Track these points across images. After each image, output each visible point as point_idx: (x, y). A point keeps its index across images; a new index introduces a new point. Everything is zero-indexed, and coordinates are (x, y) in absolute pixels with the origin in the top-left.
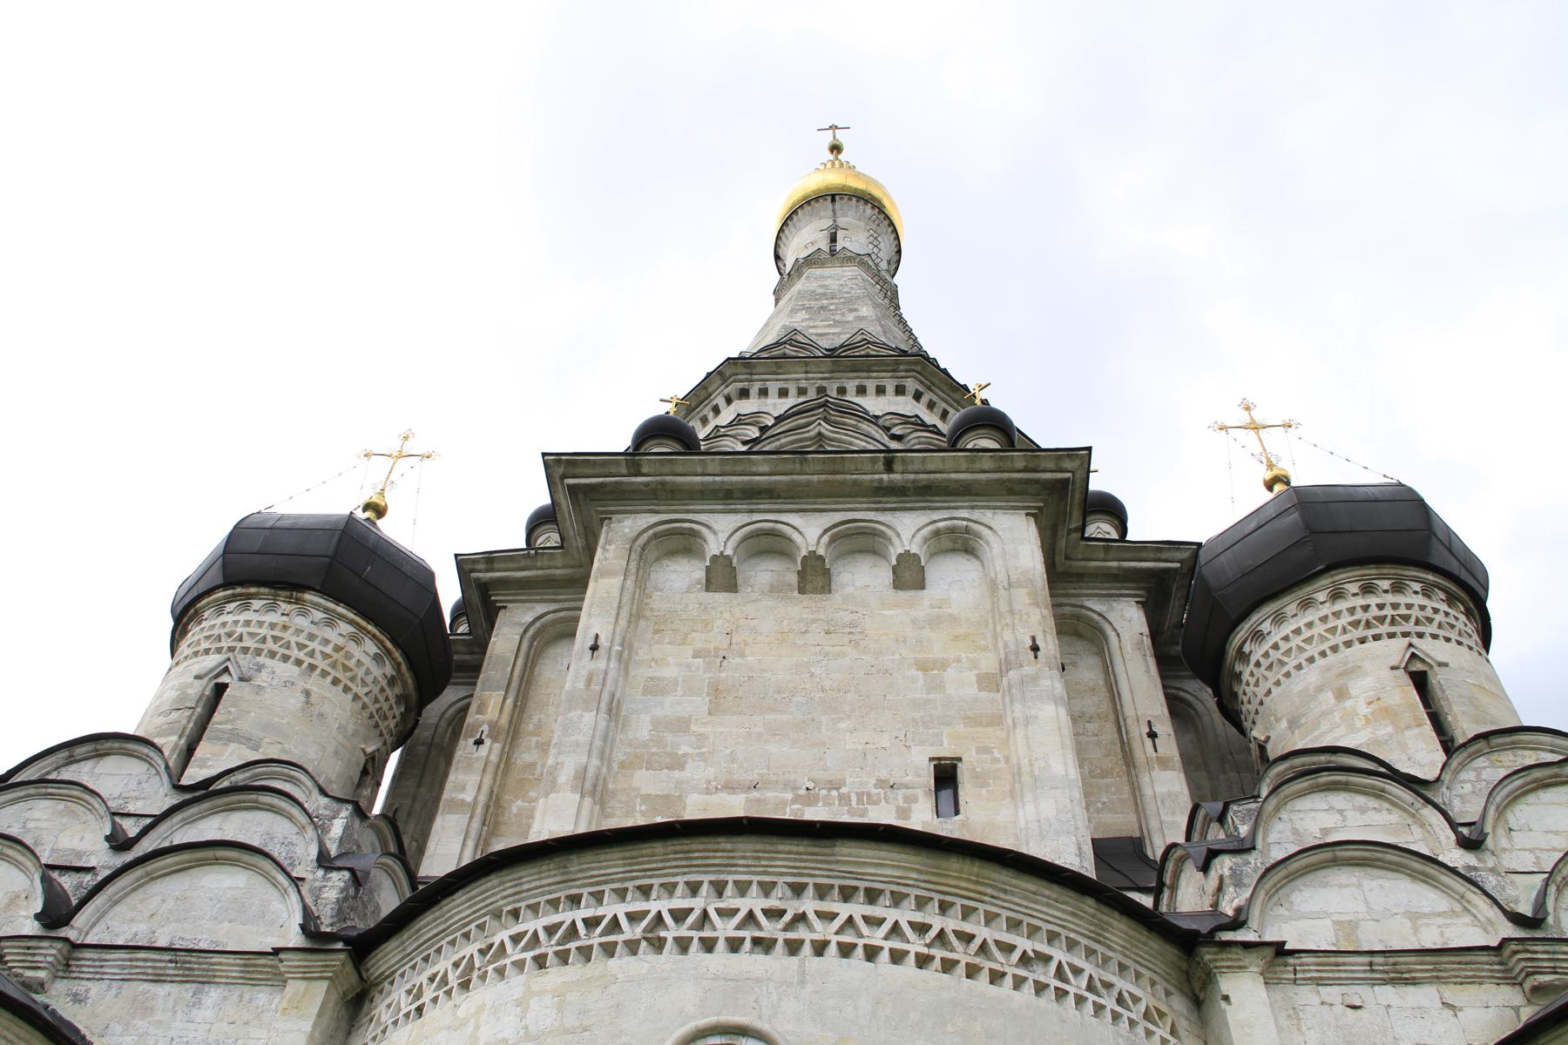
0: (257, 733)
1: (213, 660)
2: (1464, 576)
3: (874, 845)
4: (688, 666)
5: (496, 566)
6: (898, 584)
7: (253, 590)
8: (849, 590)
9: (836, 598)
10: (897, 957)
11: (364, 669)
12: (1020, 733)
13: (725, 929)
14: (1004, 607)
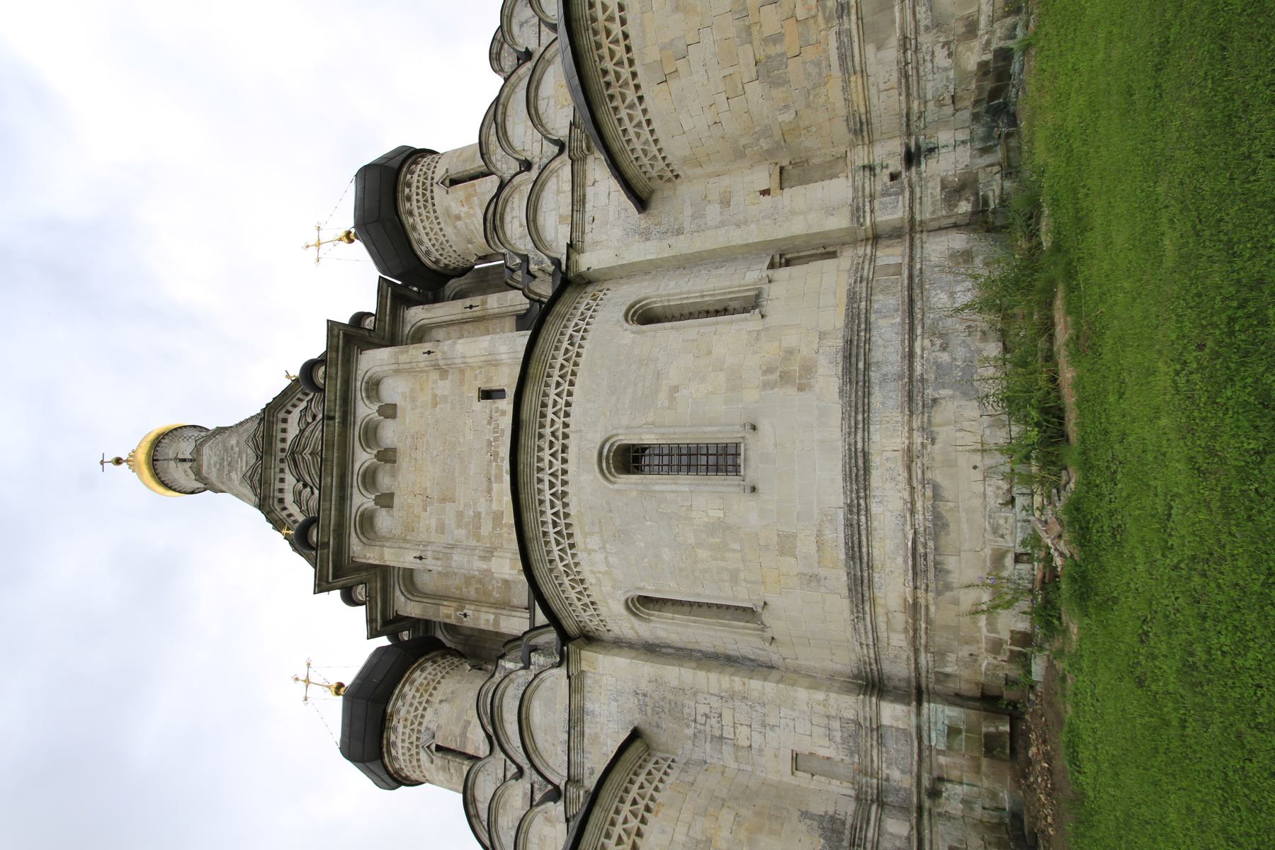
0: (462, 724)
1: (424, 756)
2: (404, 155)
6: (393, 416)
8: (395, 439)
9: (399, 445)
10: (570, 394)
12: (468, 360)
13: (558, 465)
14: (408, 366)
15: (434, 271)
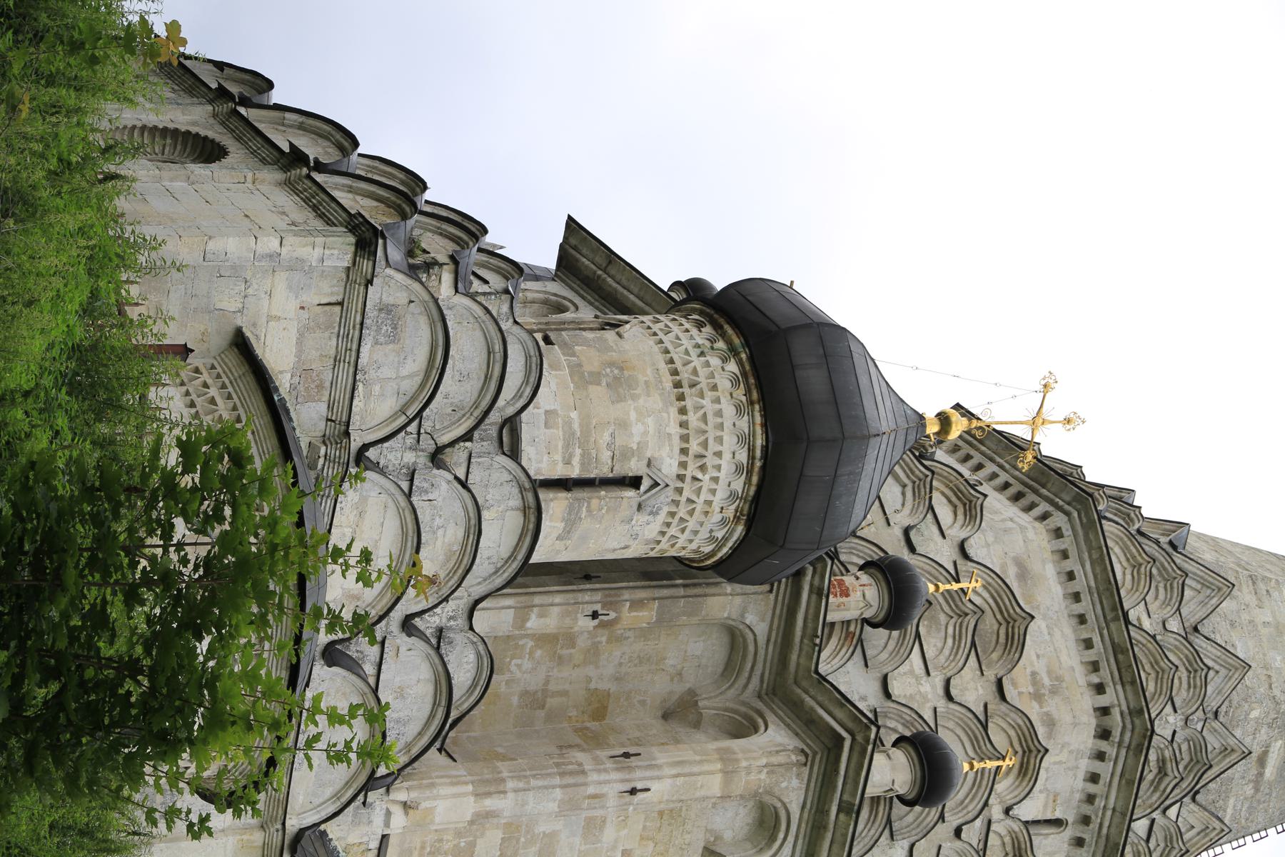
1: (669, 466)
4: (614, 848)
5: (814, 597)
7: (755, 479)
11: (717, 461)
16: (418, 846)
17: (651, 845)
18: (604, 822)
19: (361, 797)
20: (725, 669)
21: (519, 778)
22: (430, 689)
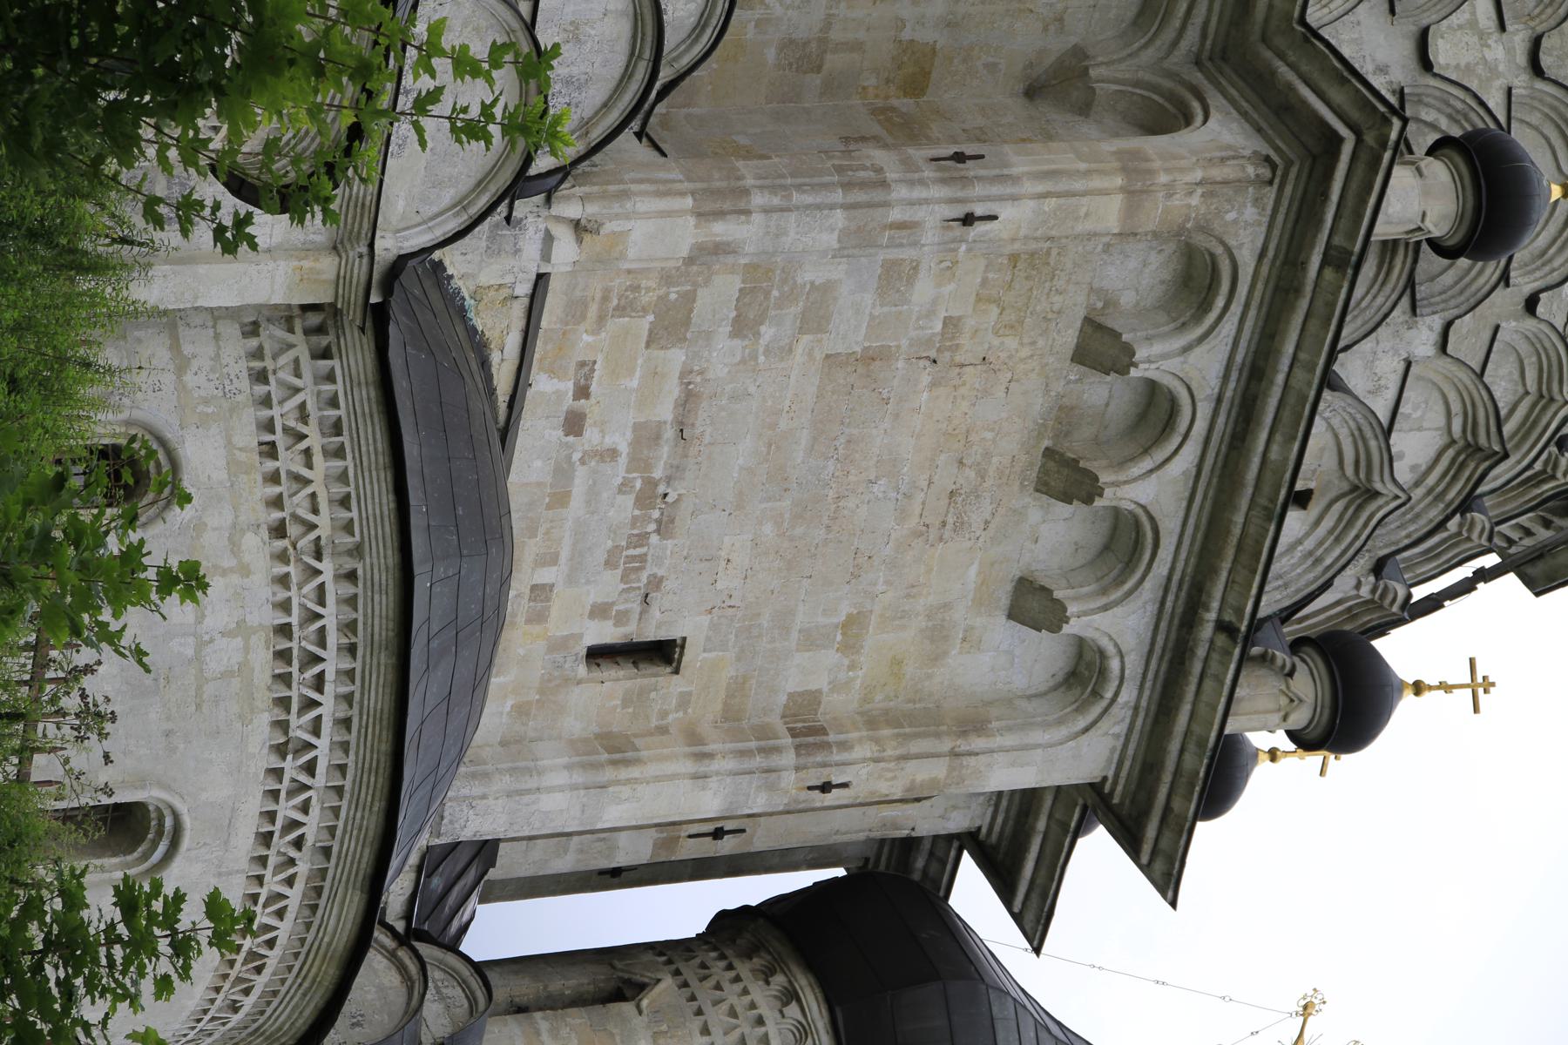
3: (359, 920)
4: (930, 314)
8: (1034, 515)
12: (689, 767)
15: (813, 967)
16: (598, 296)
17: (995, 310)
18: (916, 269)
19: (502, 209)
20: (1141, 13)
21: (773, 189)
22: (624, 28)
